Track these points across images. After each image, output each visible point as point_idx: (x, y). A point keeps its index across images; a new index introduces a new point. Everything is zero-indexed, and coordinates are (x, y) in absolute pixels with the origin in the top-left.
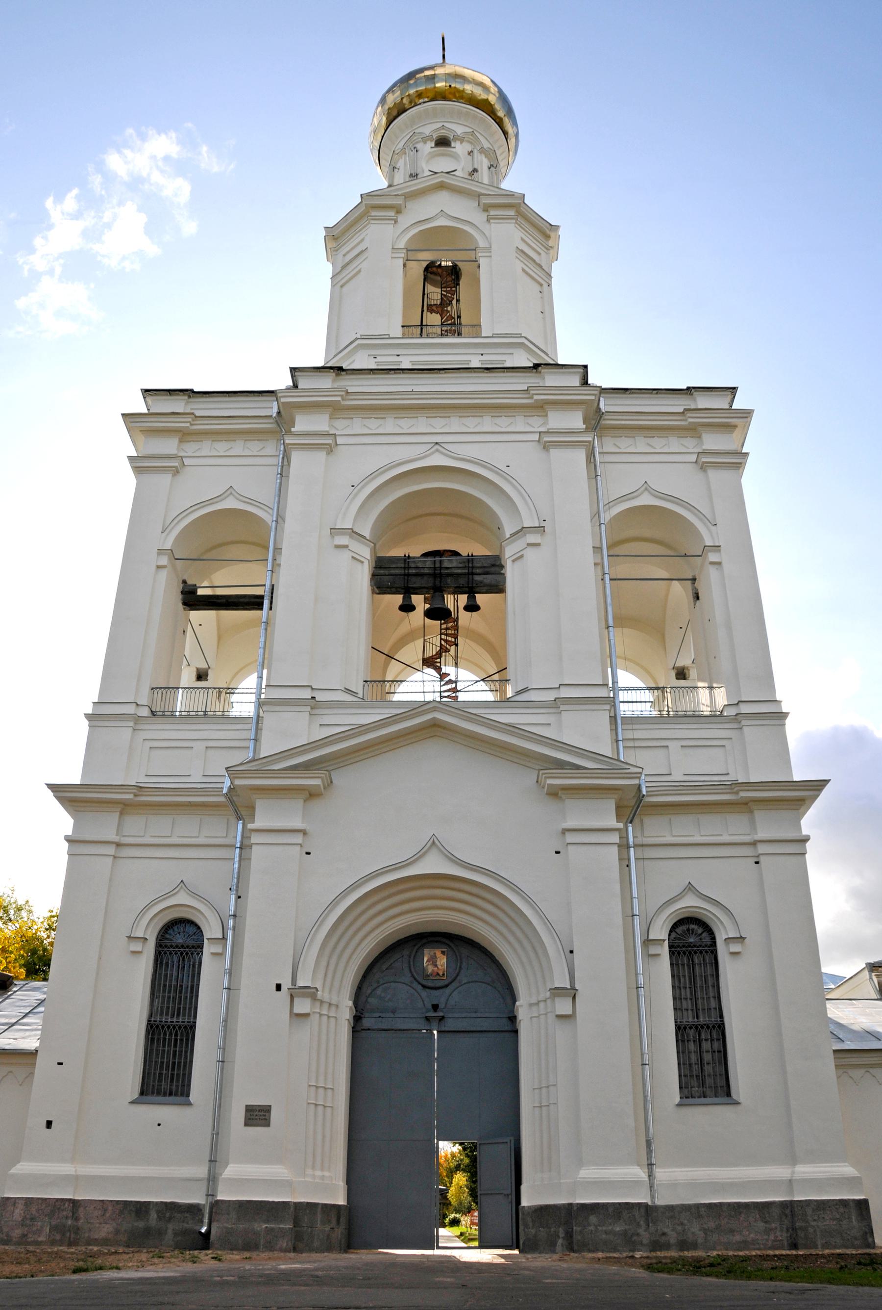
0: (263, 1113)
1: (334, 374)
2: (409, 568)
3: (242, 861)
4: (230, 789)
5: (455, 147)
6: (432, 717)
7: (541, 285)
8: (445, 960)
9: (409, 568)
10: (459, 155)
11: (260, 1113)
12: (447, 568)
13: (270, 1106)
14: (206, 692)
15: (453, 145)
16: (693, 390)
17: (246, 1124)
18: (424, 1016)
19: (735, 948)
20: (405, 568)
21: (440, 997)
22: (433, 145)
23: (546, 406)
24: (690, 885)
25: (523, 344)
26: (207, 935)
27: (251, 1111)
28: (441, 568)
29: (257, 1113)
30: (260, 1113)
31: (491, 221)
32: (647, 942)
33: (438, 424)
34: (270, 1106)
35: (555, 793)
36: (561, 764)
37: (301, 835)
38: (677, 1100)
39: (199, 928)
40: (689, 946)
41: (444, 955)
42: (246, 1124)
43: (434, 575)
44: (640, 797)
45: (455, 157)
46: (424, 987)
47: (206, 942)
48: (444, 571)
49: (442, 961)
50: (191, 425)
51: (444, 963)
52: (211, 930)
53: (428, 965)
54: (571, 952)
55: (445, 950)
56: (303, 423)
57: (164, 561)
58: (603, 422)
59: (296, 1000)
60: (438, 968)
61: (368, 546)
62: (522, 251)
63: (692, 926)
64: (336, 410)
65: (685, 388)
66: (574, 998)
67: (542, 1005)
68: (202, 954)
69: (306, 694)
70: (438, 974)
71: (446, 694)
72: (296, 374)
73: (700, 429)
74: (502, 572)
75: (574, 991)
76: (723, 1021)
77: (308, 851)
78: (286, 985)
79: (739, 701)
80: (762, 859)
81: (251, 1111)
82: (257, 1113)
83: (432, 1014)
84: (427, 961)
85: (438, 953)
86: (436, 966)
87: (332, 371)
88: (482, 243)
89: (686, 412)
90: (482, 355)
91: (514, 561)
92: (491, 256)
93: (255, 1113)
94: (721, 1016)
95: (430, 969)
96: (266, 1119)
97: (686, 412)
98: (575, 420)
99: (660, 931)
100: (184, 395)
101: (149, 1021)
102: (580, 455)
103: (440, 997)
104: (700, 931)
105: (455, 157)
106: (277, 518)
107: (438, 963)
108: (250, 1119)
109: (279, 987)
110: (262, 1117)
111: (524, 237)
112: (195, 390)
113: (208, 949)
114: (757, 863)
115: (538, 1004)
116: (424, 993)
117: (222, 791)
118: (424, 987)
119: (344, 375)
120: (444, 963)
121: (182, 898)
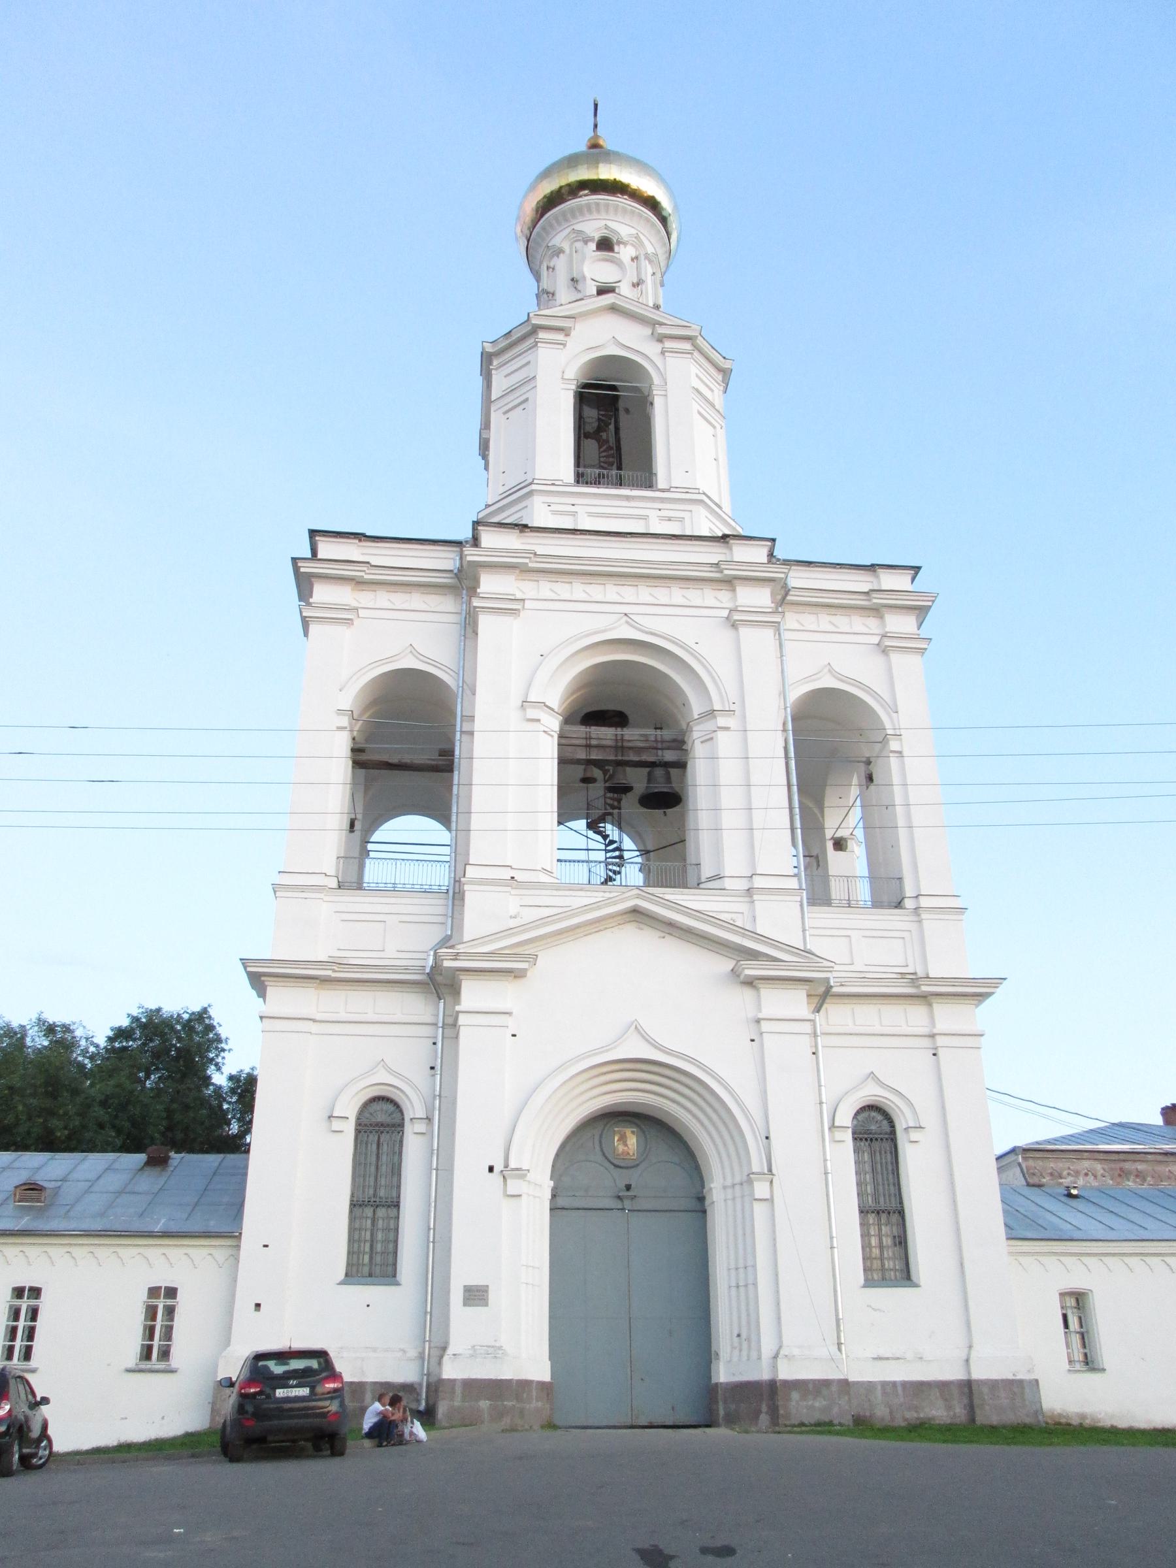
1: (518, 531)
2: (590, 738)
3: (445, 1040)
4: (432, 968)
5: (619, 253)
6: (634, 904)
7: (714, 427)
8: (635, 1140)
9: (590, 738)
10: (624, 264)
11: (477, 1294)
12: (629, 741)
13: (487, 1286)
14: (394, 863)
15: (616, 248)
16: (877, 567)
17: (465, 1304)
19: (914, 1135)
20: (586, 738)
21: (633, 1177)
22: (595, 249)
23: (736, 582)
24: (872, 1075)
25: (702, 501)
26: (408, 1115)
28: (622, 740)
31: (666, 354)
32: (833, 1127)
33: (628, 593)
34: (487, 1286)
35: (750, 983)
36: (754, 955)
38: (862, 1281)
39: (396, 1105)
40: (870, 1133)
42: (465, 1304)
43: (616, 748)
44: (829, 988)
45: (619, 263)
46: (616, 1166)
48: (626, 744)
49: (632, 1141)
51: (634, 1143)
52: (414, 1108)
53: (618, 1144)
54: (767, 1138)
55: (635, 1130)
56: (489, 584)
57: (345, 721)
58: (789, 598)
59: (509, 1181)
60: (628, 1148)
61: (556, 718)
62: (697, 390)
63: (873, 1114)
65: (869, 564)
66: (771, 1182)
67: (737, 1188)
68: (403, 1133)
69: (506, 874)
70: (628, 1154)
72: (479, 528)
73: (884, 609)
74: (684, 747)
75: (771, 1176)
76: (903, 1207)
77: (514, 1033)
79: (919, 895)
80: (941, 1052)
83: (624, 1193)
84: (618, 1140)
85: (628, 1132)
86: (626, 1145)
87: (516, 528)
88: (656, 380)
89: (871, 593)
90: (660, 510)
91: (702, 742)
92: (666, 395)
94: (901, 1203)
95: (621, 1148)
96: (485, 1299)
97: (871, 593)
99: (845, 1118)
100: (355, 538)
101: (352, 1201)
103: (633, 1177)
104: (879, 1117)
105: (619, 263)
106: (463, 685)
107: (628, 1143)
108: (468, 1299)
109: (491, 1169)
110: (481, 1297)
111: (700, 374)
112: (367, 534)
113: (409, 1129)
114: (934, 1055)
115: (733, 1186)
116: (616, 1172)
117: (425, 970)
118: (616, 1166)
119: (528, 532)
120: (634, 1143)
121: (383, 1077)
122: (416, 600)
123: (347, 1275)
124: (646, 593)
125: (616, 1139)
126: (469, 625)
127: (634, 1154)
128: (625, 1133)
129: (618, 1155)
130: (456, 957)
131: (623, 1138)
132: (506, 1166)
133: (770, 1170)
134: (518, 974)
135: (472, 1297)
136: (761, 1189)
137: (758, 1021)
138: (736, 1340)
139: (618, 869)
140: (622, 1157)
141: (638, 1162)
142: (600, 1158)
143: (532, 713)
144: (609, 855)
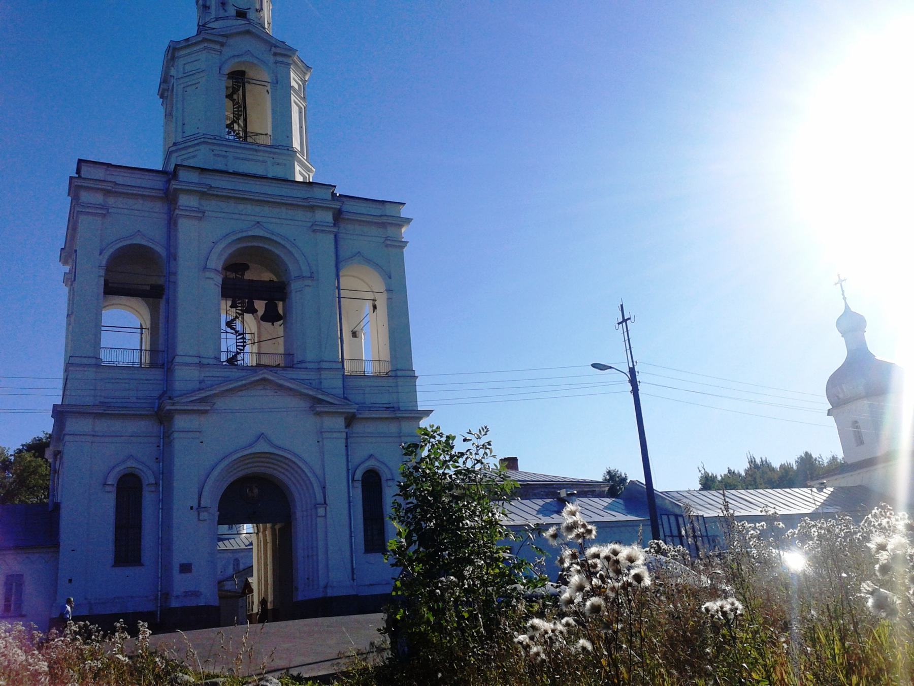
32: (353, 480)
35: (319, 414)
36: (321, 401)
37: (198, 433)
47: (144, 486)
50: (113, 188)
52: (148, 478)
64: (203, 195)
69: (196, 360)
71: (240, 344)
78: (195, 505)
98: (329, 217)
99: (359, 475)
102: (332, 237)
109: (192, 508)
121: (130, 464)
122: (139, 204)
123: (115, 562)
124: (267, 210)
126: (171, 223)
130: (173, 404)
132: (199, 506)
133: (325, 503)
134: (205, 412)
136: (321, 511)
137: (321, 432)
138: (307, 580)
139: (242, 348)
143: (208, 274)
144: (238, 341)
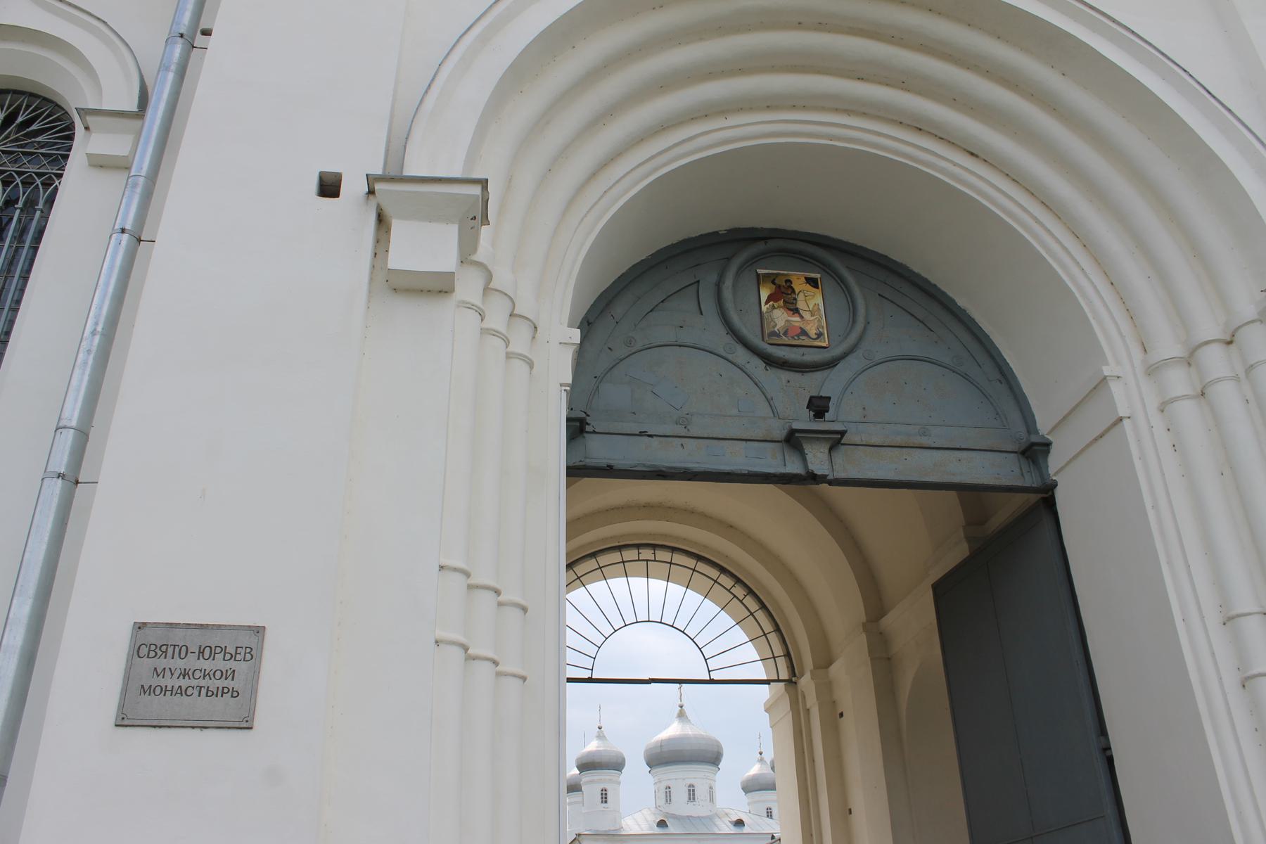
0: (219, 663)
8: (819, 300)
11: (207, 665)
13: (259, 631)
18: (780, 434)
27: (160, 650)
29: (192, 662)
30: (207, 665)
41: (817, 287)
46: (772, 362)
49: (812, 301)
55: (818, 276)
60: (802, 317)
70: (804, 333)
81: (160, 650)
82: (192, 662)
84: (767, 303)
86: (796, 311)
93: (179, 664)
96: (235, 694)
107: (801, 304)
108: (146, 690)
110: (214, 684)
116: (775, 380)
125: (765, 294)
127: (820, 335)
128: (789, 281)
129: (773, 334)
131: (784, 295)
135: (168, 682)
140: (785, 340)
141: (837, 352)
142: (718, 337)
